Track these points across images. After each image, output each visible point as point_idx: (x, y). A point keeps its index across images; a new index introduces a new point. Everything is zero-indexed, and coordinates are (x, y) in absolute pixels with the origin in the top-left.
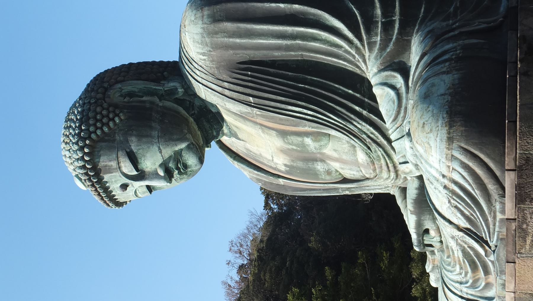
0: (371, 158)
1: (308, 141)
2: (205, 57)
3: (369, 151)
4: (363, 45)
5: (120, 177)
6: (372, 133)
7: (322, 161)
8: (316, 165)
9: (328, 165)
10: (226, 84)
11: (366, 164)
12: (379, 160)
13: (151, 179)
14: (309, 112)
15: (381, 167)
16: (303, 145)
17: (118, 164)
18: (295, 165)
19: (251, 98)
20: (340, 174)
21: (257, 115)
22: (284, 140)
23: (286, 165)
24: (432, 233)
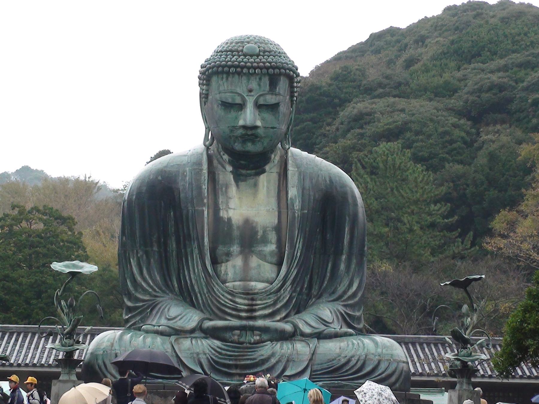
0: (262, 293)
1: (272, 247)
2: (328, 182)
3: (268, 293)
4: (343, 301)
5: (264, 91)
6: (284, 298)
7: (241, 252)
8: (238, 246)
9: (237, 256)
10: (312, 193)
11: (250, 288)
12: (261, 300)
13: (254, 115)
14: (299, 254)
15: (253, 299)
16: (265, 241)
17: (276, 95)
18: (235, 227)
19: (306, 211)
20: (222, 262)
21: (294, 213)
22: (268, 227)
23: (229, 219)
24: (258, 338)
